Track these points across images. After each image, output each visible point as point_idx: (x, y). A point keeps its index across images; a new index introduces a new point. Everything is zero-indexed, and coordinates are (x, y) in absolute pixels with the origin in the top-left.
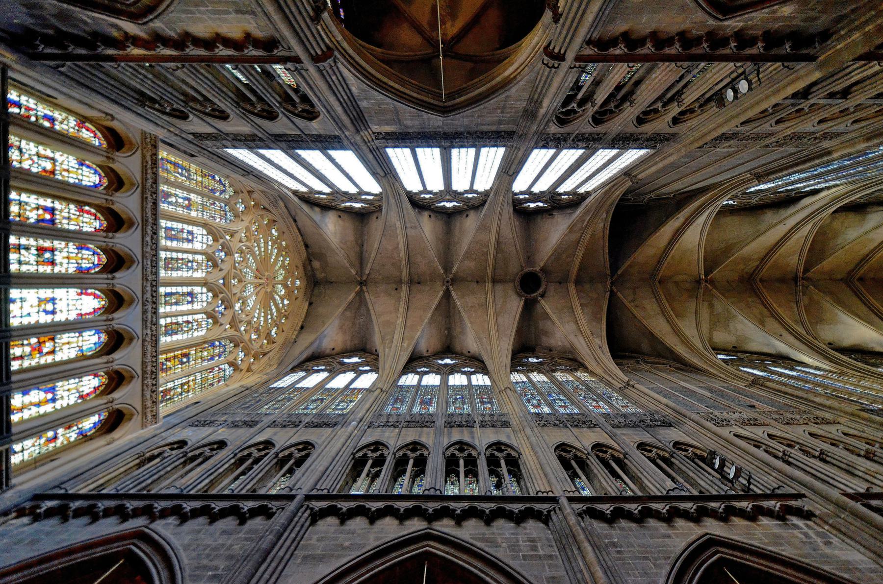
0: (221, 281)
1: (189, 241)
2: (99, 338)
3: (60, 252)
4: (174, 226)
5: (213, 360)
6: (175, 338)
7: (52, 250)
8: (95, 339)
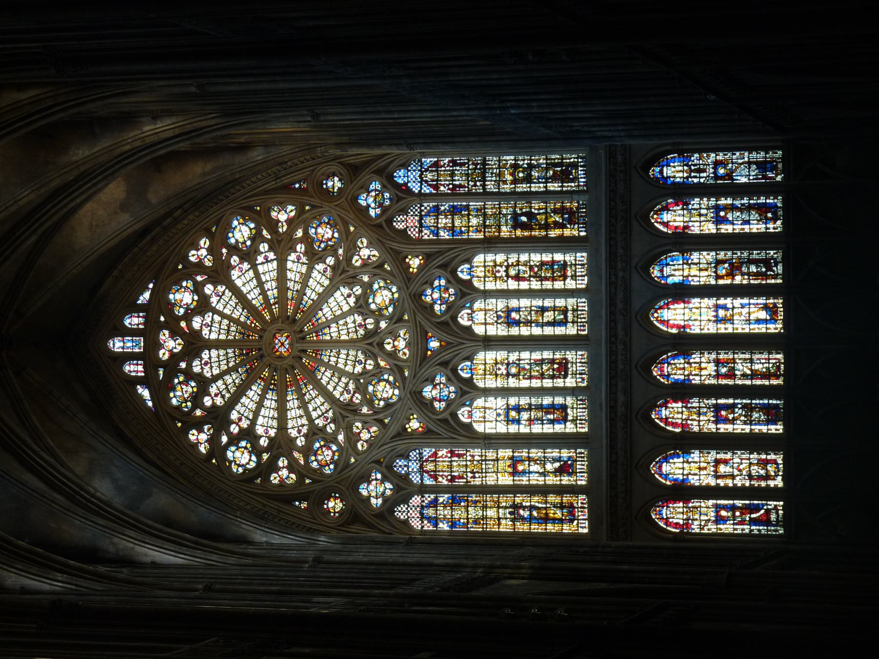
0: (434, 344)
1: (518, 409)
2: (661, 271)
3: (710, 375)
4: (545, 426)
5: (453, 207)
6: (547, 257)
7: (718, 376)
8: (667, 271)
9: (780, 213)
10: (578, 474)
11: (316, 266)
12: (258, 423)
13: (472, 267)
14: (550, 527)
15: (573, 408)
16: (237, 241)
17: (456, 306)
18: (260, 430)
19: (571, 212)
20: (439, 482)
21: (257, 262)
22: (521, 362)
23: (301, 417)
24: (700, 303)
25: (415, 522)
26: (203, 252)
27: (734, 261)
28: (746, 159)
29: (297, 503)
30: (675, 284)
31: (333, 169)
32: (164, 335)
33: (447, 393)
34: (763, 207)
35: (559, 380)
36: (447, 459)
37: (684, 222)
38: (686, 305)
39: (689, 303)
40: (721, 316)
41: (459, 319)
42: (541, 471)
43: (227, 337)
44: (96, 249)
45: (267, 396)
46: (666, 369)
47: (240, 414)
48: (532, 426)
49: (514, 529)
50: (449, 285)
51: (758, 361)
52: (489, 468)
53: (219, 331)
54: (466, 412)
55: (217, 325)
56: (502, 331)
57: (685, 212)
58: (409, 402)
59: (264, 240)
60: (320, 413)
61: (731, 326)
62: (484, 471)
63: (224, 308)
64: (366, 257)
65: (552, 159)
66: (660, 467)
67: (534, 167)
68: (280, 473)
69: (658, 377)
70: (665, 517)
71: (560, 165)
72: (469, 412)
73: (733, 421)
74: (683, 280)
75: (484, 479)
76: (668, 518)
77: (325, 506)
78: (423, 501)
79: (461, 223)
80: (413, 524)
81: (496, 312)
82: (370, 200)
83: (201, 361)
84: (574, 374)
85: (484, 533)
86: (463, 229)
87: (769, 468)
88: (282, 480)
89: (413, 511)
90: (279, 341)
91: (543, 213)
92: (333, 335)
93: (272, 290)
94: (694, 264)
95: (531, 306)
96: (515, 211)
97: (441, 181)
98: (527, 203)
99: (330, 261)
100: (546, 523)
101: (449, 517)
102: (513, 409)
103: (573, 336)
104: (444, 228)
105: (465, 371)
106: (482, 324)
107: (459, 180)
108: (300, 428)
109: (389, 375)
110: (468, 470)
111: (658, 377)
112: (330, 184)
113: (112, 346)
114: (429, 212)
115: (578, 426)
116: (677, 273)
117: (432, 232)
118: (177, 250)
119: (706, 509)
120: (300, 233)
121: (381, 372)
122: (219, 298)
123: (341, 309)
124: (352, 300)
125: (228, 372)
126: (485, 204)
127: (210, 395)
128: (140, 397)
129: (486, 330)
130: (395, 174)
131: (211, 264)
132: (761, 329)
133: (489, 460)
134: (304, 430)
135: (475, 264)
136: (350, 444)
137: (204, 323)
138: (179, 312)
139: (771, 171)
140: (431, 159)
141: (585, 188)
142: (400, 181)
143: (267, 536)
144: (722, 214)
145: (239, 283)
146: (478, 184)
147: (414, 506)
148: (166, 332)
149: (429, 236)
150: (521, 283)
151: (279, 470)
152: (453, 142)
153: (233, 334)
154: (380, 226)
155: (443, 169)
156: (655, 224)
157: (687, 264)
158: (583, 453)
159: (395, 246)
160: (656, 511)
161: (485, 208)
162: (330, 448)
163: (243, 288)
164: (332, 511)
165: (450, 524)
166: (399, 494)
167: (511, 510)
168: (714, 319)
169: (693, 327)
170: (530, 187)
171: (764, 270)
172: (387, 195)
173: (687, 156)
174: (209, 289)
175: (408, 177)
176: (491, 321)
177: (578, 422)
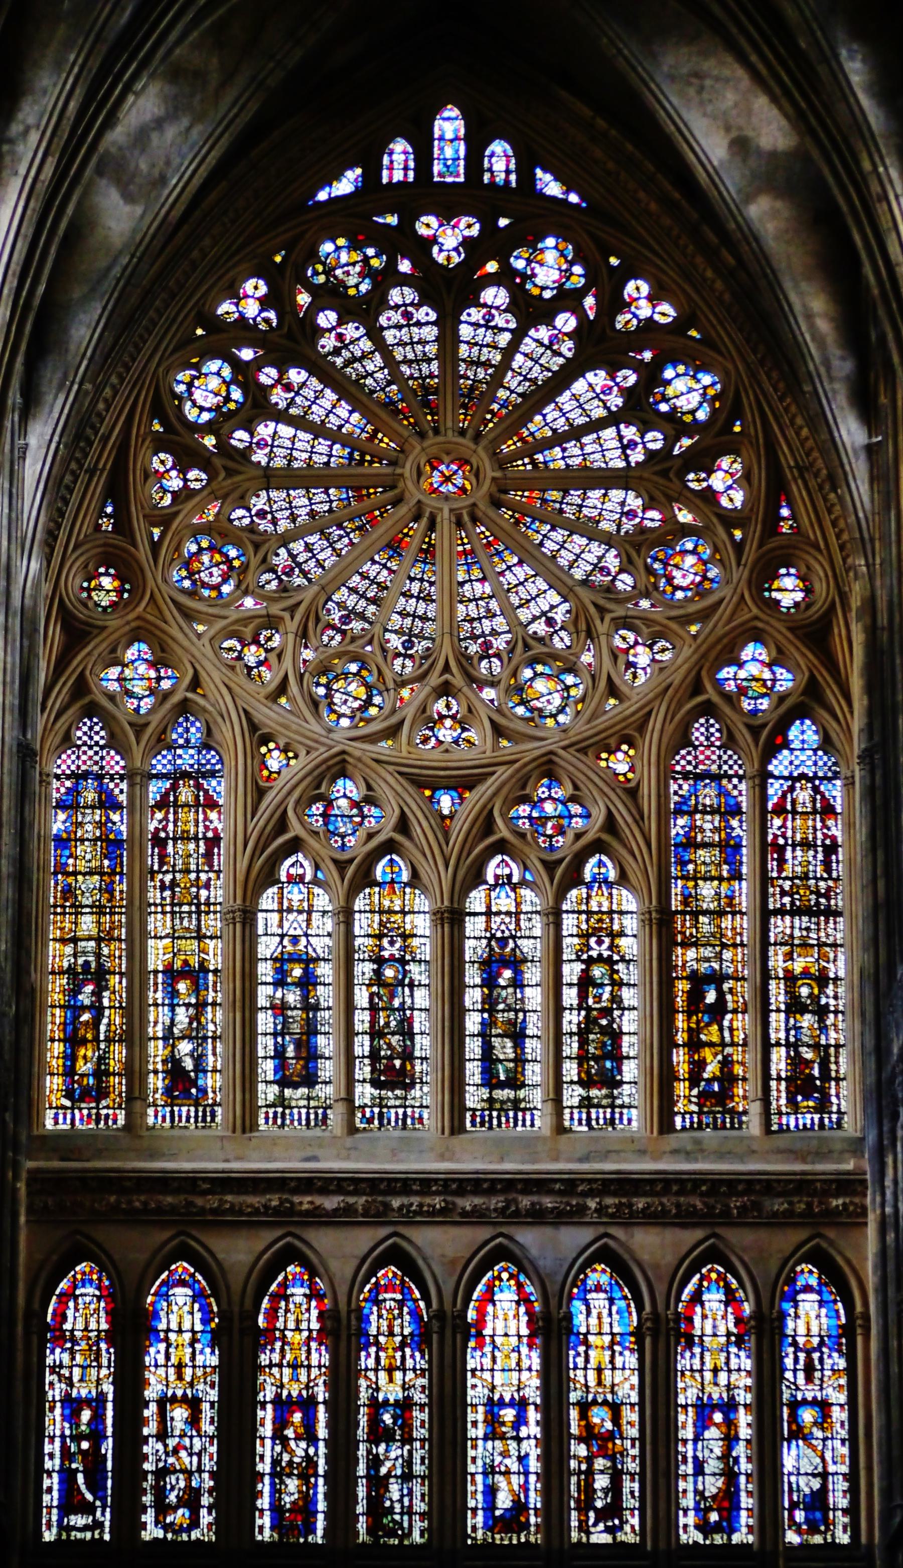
0: (446, 802)
1: (308, 982)
2: (598, 1288)
3: (378, 1389)
4: (270, 1041)
5: (738, 846)
6: (629, 1045)
7: (376, 1406)
8: (598, 1301)
9: (718, 1539)
10: (168, 1109)
11: (613, 552)
12: (280, 426)
13: (610, 885)
14: (58, 1048)
15: (309, 1098)
16: (668, 382)
17: (527, 850)
18: (265, 430)
19: (725, 1096)
20: (153, 813)
21: (622, 426)
22: (407, 990)
23: (293, 518)
24: (530, 1369)
25: (69, 762)
26: (644, 310)
27: (618, 1442)
28: (831, 1468)
29: (109, 510)
30: (569, 1317)
31: (820, 587)
32: (469, 226)
33: (342, 830)
34: (731, 1502)
35: (368, 1069)
36: (201, 829)
37: (701, 1337)
38: (525, 1340)
39: (530, 1346)
40: (502, 1413)
41: (499, 858)
42: (176, 1031)
43: (464, 360)
44: (653, 86)
45: (337, 447)
46: (390, 1298)
47: (300, 388)
48: (270, 1012)
49: (53, 973)
50: (570, 835)
51: (405, 1492)
52: (182, 919)
53: (476, 344)
54: (300, 871)
55: (489, 339)
56: (473, 949)
57: (723, 1340)
58: (322, 749)
59: (670, 441)
60: (300, 559)
61: (480, 1432)
62: (177, 909)
63: (526, 355)
64: (631, 659)
65: (837, 1057)
66: (182, 1283)
67: (821, 1021)
68: (174, 473)
69: (373, 1280)
70: (78, 1292)
71: (825, 1075)
72: (302, 877)
73: (279, 1436)
74: (579, 1333)
75: (159, 909)
76: (76, 1298)
77: (102, 570)
78: (112, 779)
79: (704, 863)
80: (64, 757)
81: (514, 937)
82: (753, 669)
83: (412, 304)
84: (381, 1103)
85: (44, 909)
86: (691, 867)
87: (180, 1512)
88: (160, 476)
89: (90, 758)
90: (455, 473)
91: (723, 1038)
92: (467, 586)
93: (563, 458)
94: (613, 1357)
95: (525, 1012)
96: (728, 977)
97: (794, 819)
98: (745, 1003)
99: (625, 582)
100: (64, 1041)
101: (79, 834)
102: (306, 970)
103: (462, 1100)
104: (693, 827)
105: (388, 870)
106: (489, 907)
107: (795, 859)
108: (269, 517)
109: (381, 708)
110: (178, 876)
111: (373, 1280)
112: (789, 582)
113: (446, 114)
114: (728, 794)
115: (271, 1111)
116: (593, 1321)
117: (685, 800)
118: (649, 255)
119: (94, 1378)
120: (684, 517)
121: (387, 690)
122: (546, 342)
123: (521, 606)
124: (540, 628)
125: (390, 362)
126: (742, 913)
127: (341, 322)
128: (338, 176)
129: (475, 914)
130: (808, 722)
131: (619, 326)
132: (476, 1501)
133: (199, 920)
134: (264, 525)
135: (615, 891)
136: (236, 622)
137: (493, 311)
138: (517, 258)
139: (807, 1519)
140: (839, 800)
141: (775, 1127)
142: (793, 733)
143: (40, 447)
144: (718, 1417)
145: (579, 386)
146: (786, 900)
147: (102, 758)
148: (475, 231)
149: (676, 793)
150: (574, 991)
151: (179, 471)
152: (873, 850)
153: (470, 374)
154: (697, 688)
155: (819, 825)
156: (698, 1276)
157: (613, 1343)
158: (213, 1120)
159: (656, 724)
160: (91, 1273)
161: (734, 914)
162: (225, 579)
163: (567, 394)
164: (93, 584)
165: (64, 835)
166: (128, 727)
167: (93, 965)
168: (496, 1397)
169: (479, 1353)
170: (778, 1010)
171: (599, 1504)
172: (764, 704)
173: (840, 1344)
174: (566, 322)
175: (803, 749)
176: (494, 926)
177: (280, 1110)
